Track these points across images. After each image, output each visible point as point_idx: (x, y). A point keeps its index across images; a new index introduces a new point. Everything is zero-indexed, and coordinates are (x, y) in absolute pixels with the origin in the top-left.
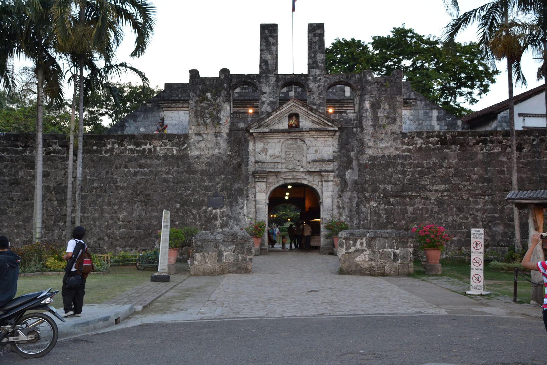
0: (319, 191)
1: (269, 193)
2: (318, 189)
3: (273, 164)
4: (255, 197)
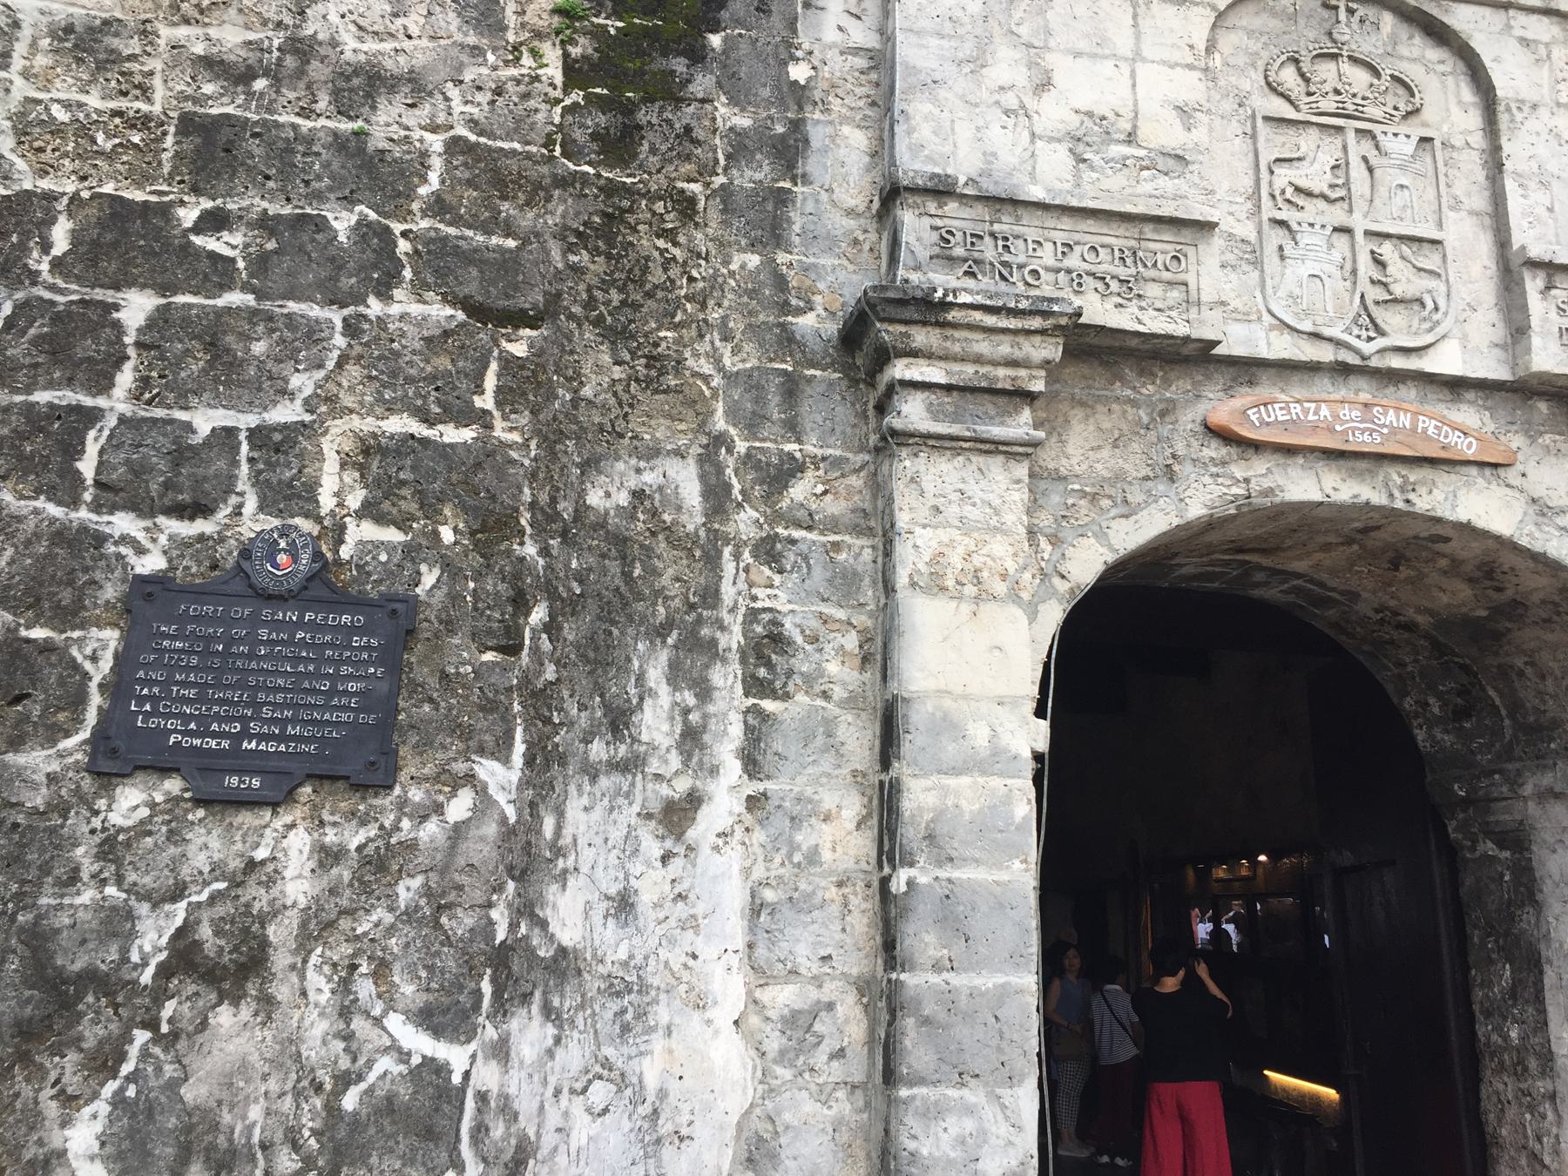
1: (1053, 616)
3: (1118, 237)
4: (879, 653)
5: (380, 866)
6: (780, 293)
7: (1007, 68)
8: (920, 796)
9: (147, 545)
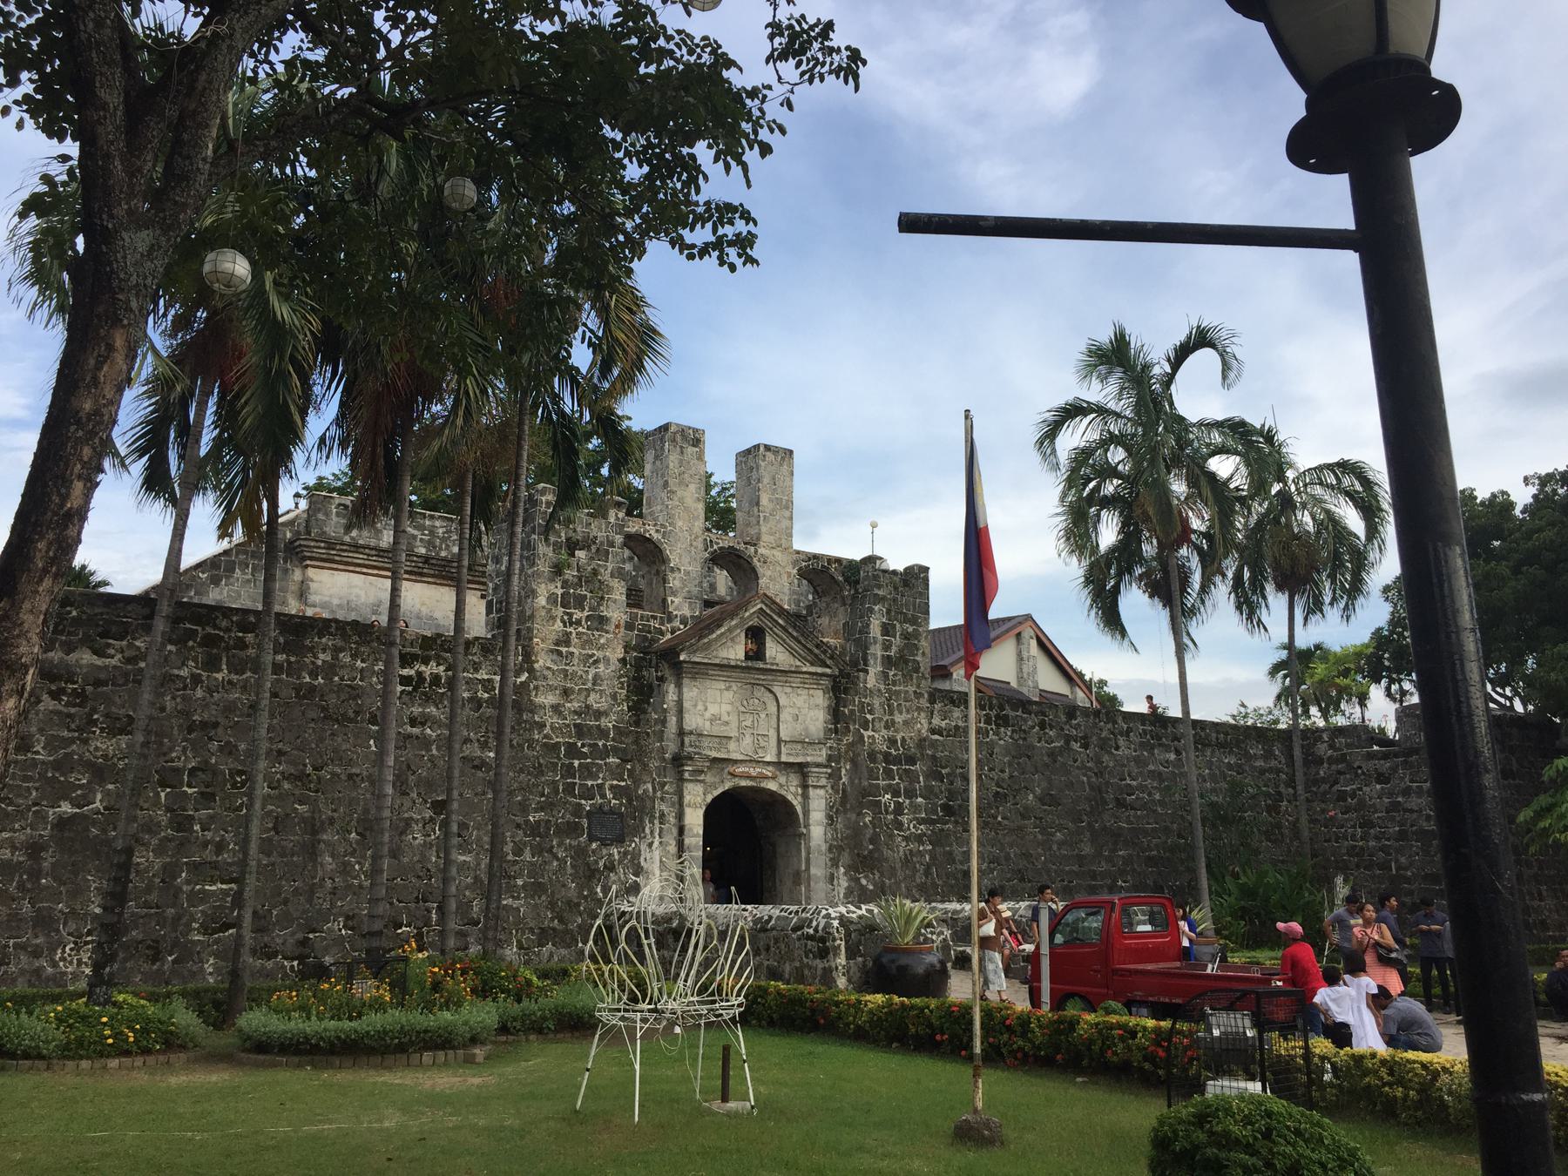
0: (799, 809)
2: (796, 803)
5: (626, 853)
6: (663, 750)
7: (700, 707)
8: (687, 841)
9: (587, 805)
